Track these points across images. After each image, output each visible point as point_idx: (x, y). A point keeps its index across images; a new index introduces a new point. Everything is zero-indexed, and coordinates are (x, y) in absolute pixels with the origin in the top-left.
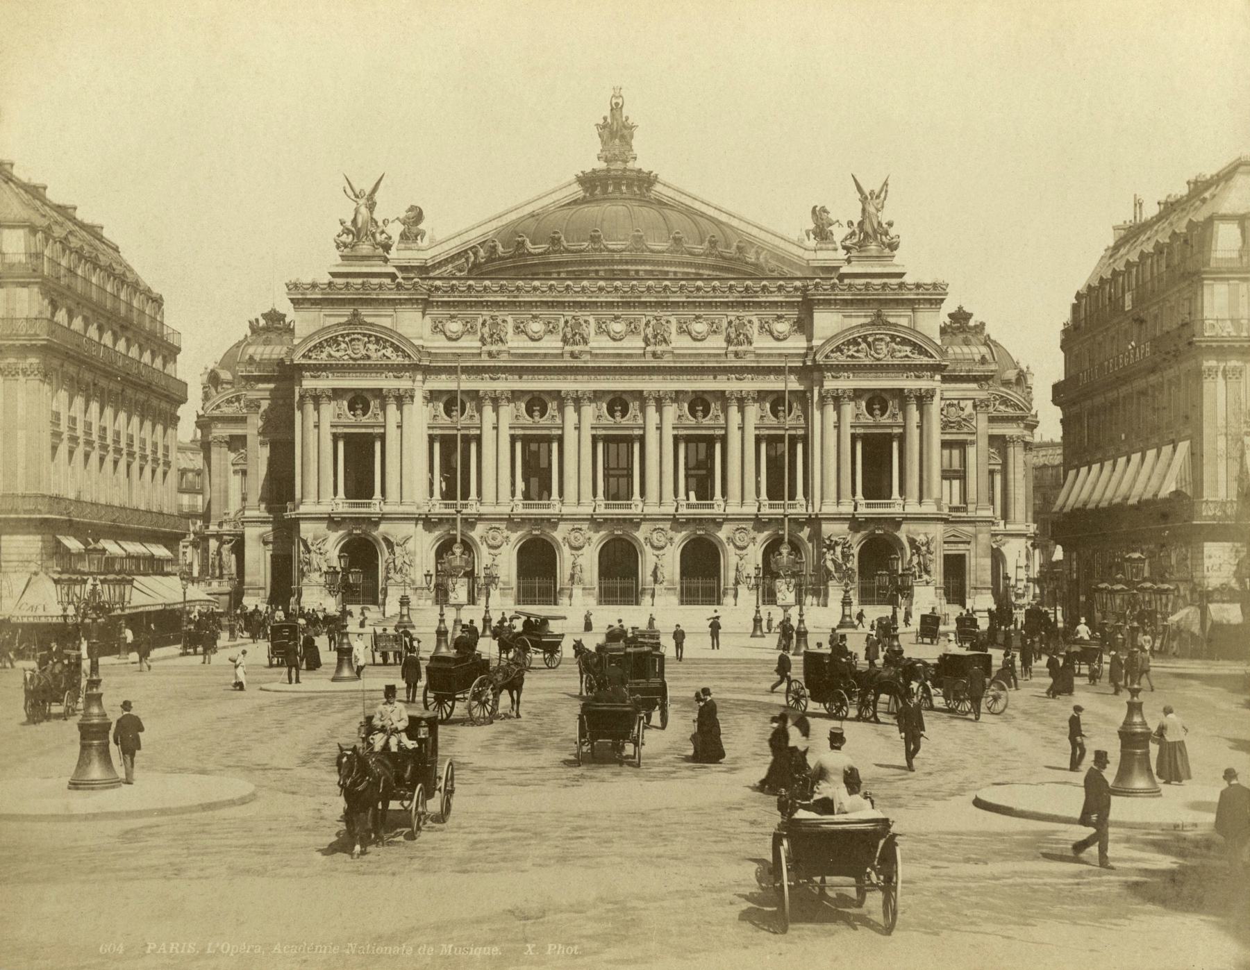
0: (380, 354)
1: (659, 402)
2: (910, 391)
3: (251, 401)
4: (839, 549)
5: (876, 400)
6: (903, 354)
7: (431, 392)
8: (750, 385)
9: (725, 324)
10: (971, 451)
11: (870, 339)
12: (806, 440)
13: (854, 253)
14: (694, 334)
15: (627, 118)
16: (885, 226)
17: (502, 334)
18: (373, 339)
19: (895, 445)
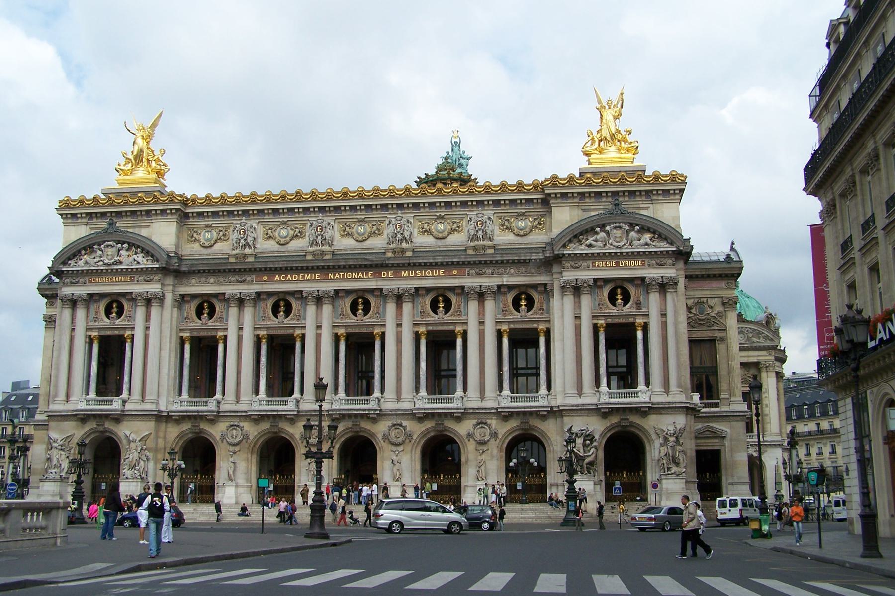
0: (131, 259)
1: (399, 299)
2: (653, 279)
3: (50, 317)
4: (579, 441)
5: (619, 290)
6: (642, 241)
7: (183, 296)
8: (489, 281)
9: (464, 223)
10: (721, 347)
11: (608, 228)
12: (548, 333)
13: (592, 156)
14: (435, 233)
15: (464, 153)
16: (624, 133)
17: (249, 240)
18: (126, 246)
19: (640, 334)
